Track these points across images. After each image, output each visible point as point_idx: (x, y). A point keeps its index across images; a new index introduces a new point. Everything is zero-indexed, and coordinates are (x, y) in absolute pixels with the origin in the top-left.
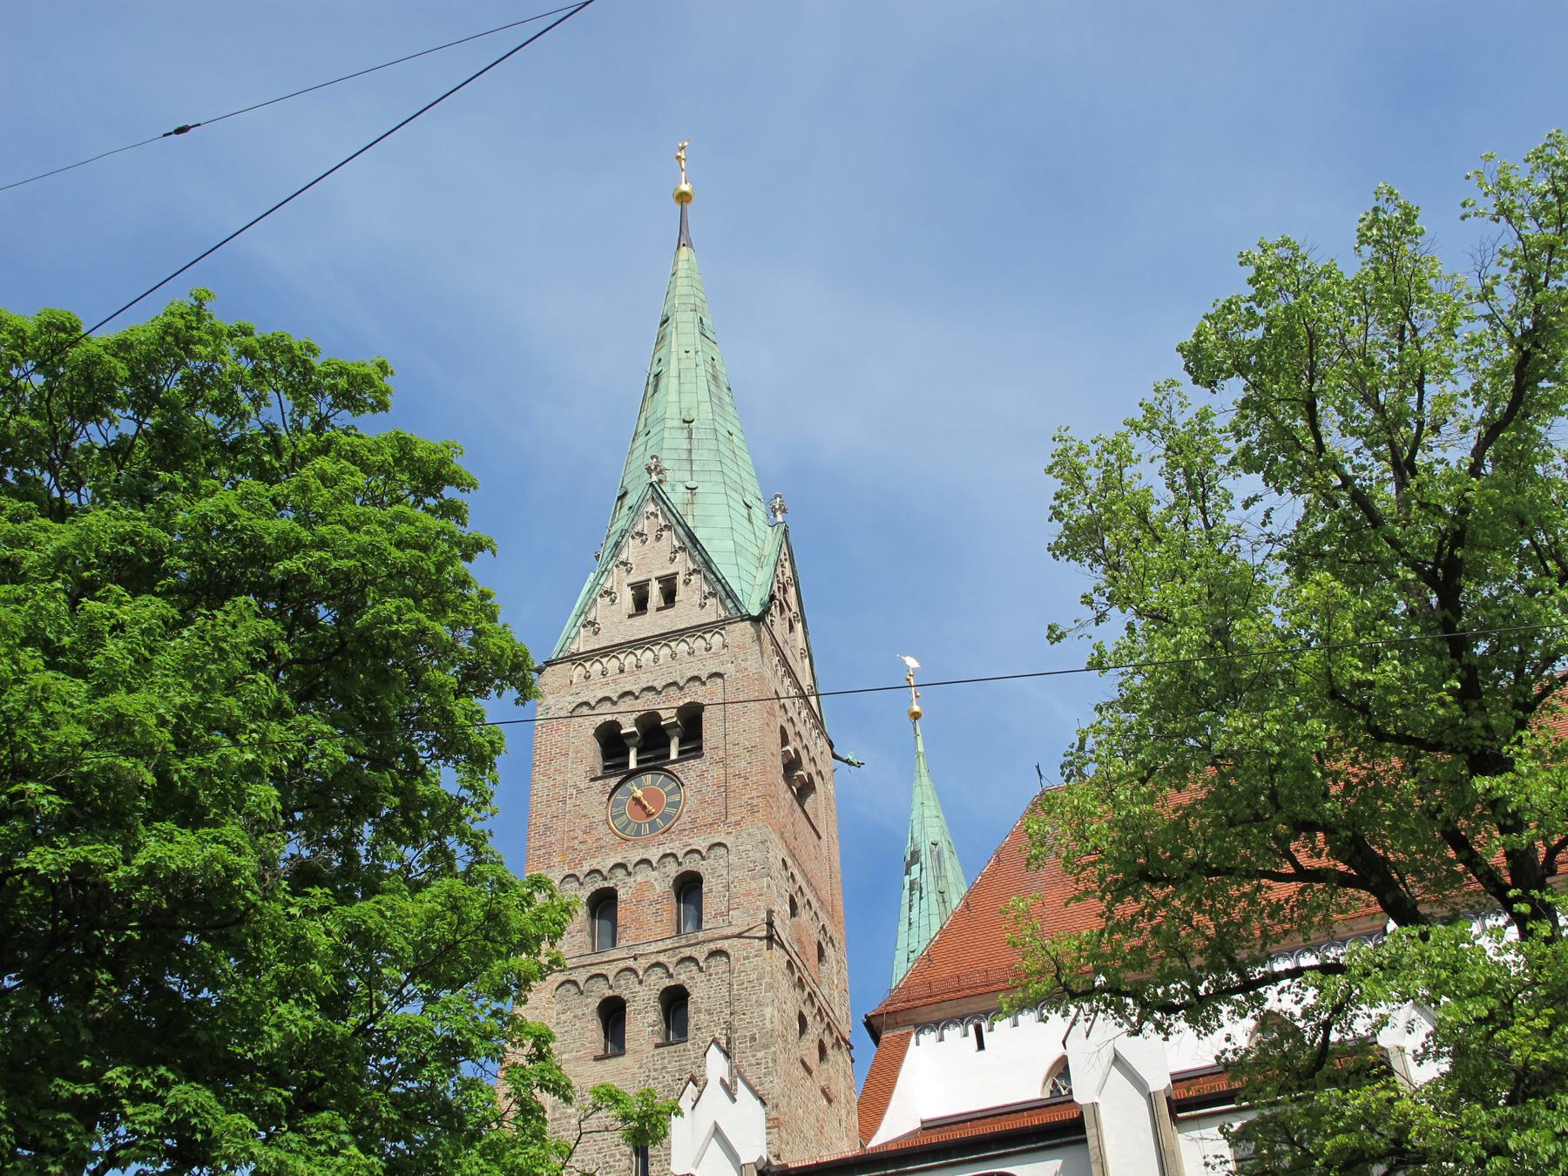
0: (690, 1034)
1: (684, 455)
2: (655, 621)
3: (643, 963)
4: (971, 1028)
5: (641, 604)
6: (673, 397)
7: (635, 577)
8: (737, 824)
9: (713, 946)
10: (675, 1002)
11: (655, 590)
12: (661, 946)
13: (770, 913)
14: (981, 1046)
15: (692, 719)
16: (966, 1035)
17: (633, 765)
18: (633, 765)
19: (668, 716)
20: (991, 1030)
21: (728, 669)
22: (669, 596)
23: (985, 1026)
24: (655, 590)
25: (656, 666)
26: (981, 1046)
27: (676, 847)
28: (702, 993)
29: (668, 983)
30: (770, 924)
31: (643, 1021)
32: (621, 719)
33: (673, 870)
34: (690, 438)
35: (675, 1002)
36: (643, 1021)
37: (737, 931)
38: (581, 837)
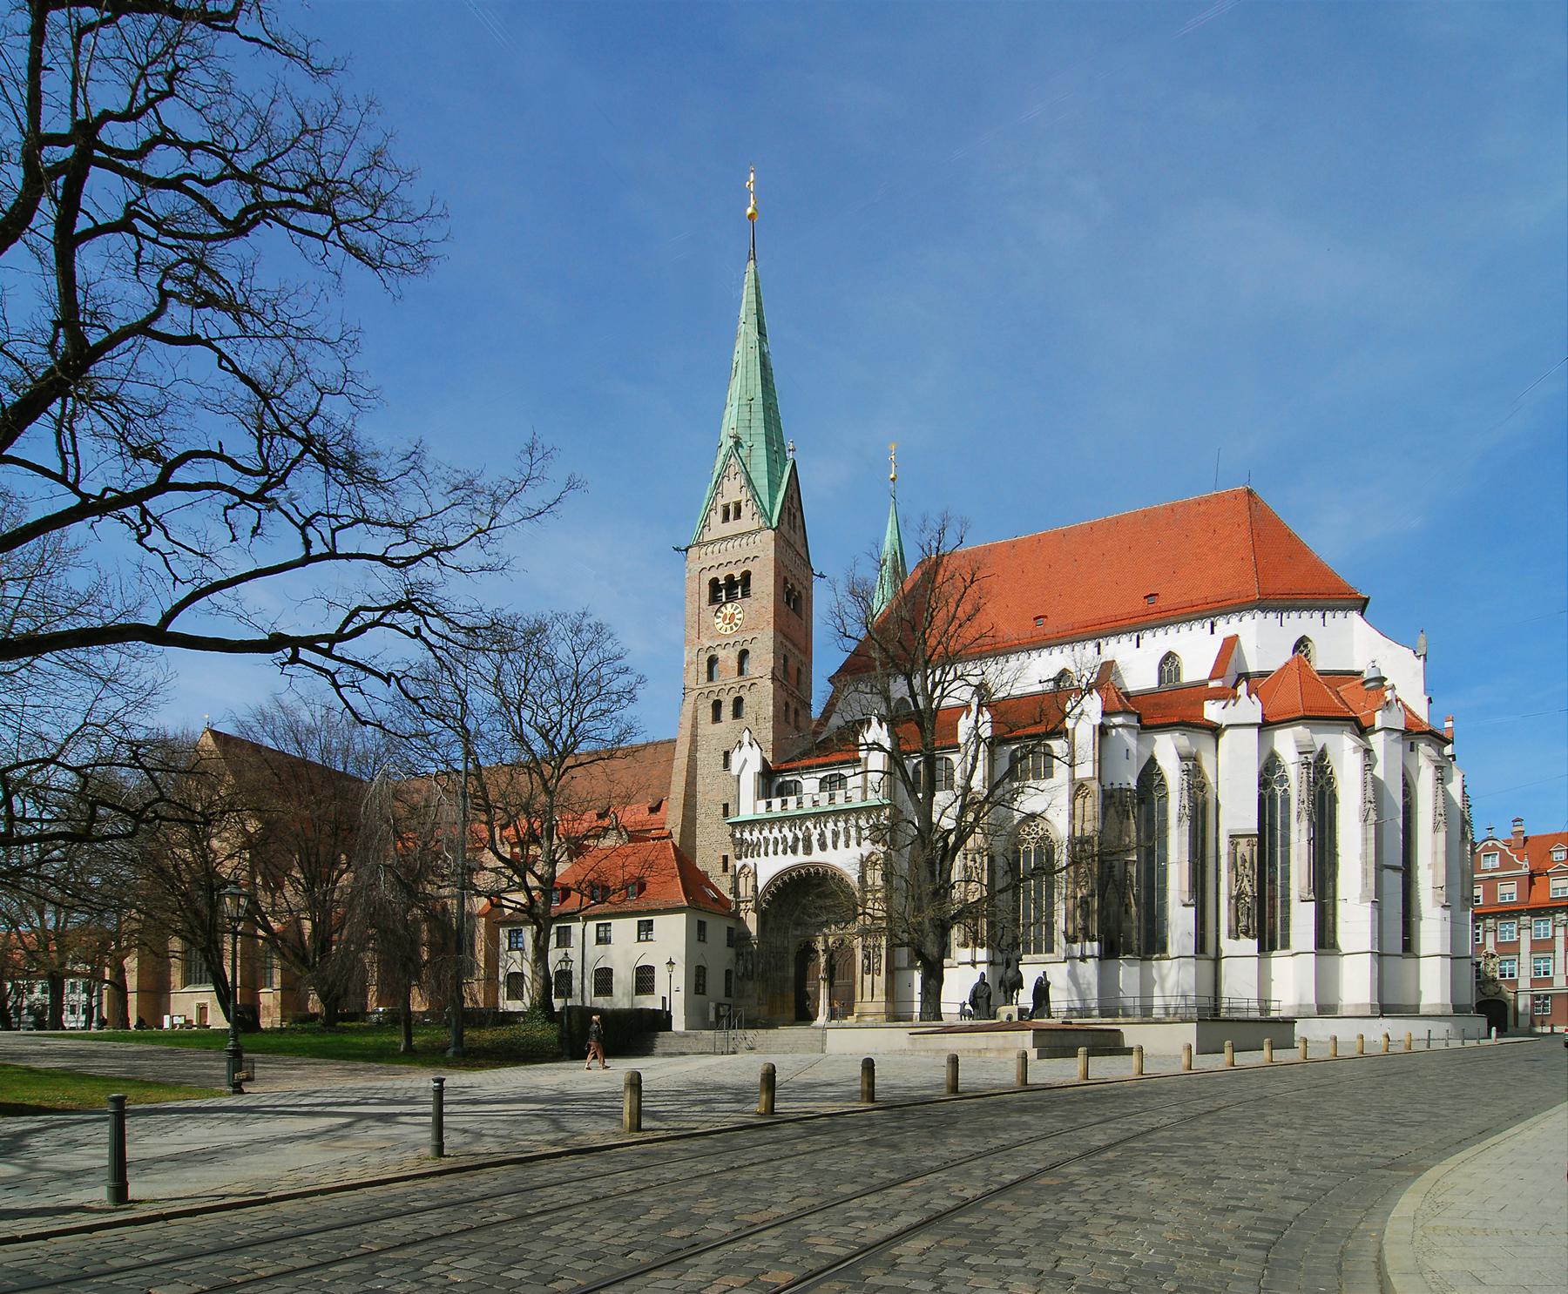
2: (733, 527)
3: (728, 687)
5: (726, 518)
7: (724, 502)
9: (752, 681)
10: (738, 702)
11: (732, 508)
12: (734, 680)
15: (747, 576)
17: (724, 600)
18: (724, 600)
19: (737, 577)
21: (761, 554)
22: (738, 515)
24: (732, 508)
25: (734, 551)
27: (739, 638)
28: (748, 700)
29: (737, 695)
31: (727, 711)
33: (739, 648)
35: (738, 702)
36: (727, 711)
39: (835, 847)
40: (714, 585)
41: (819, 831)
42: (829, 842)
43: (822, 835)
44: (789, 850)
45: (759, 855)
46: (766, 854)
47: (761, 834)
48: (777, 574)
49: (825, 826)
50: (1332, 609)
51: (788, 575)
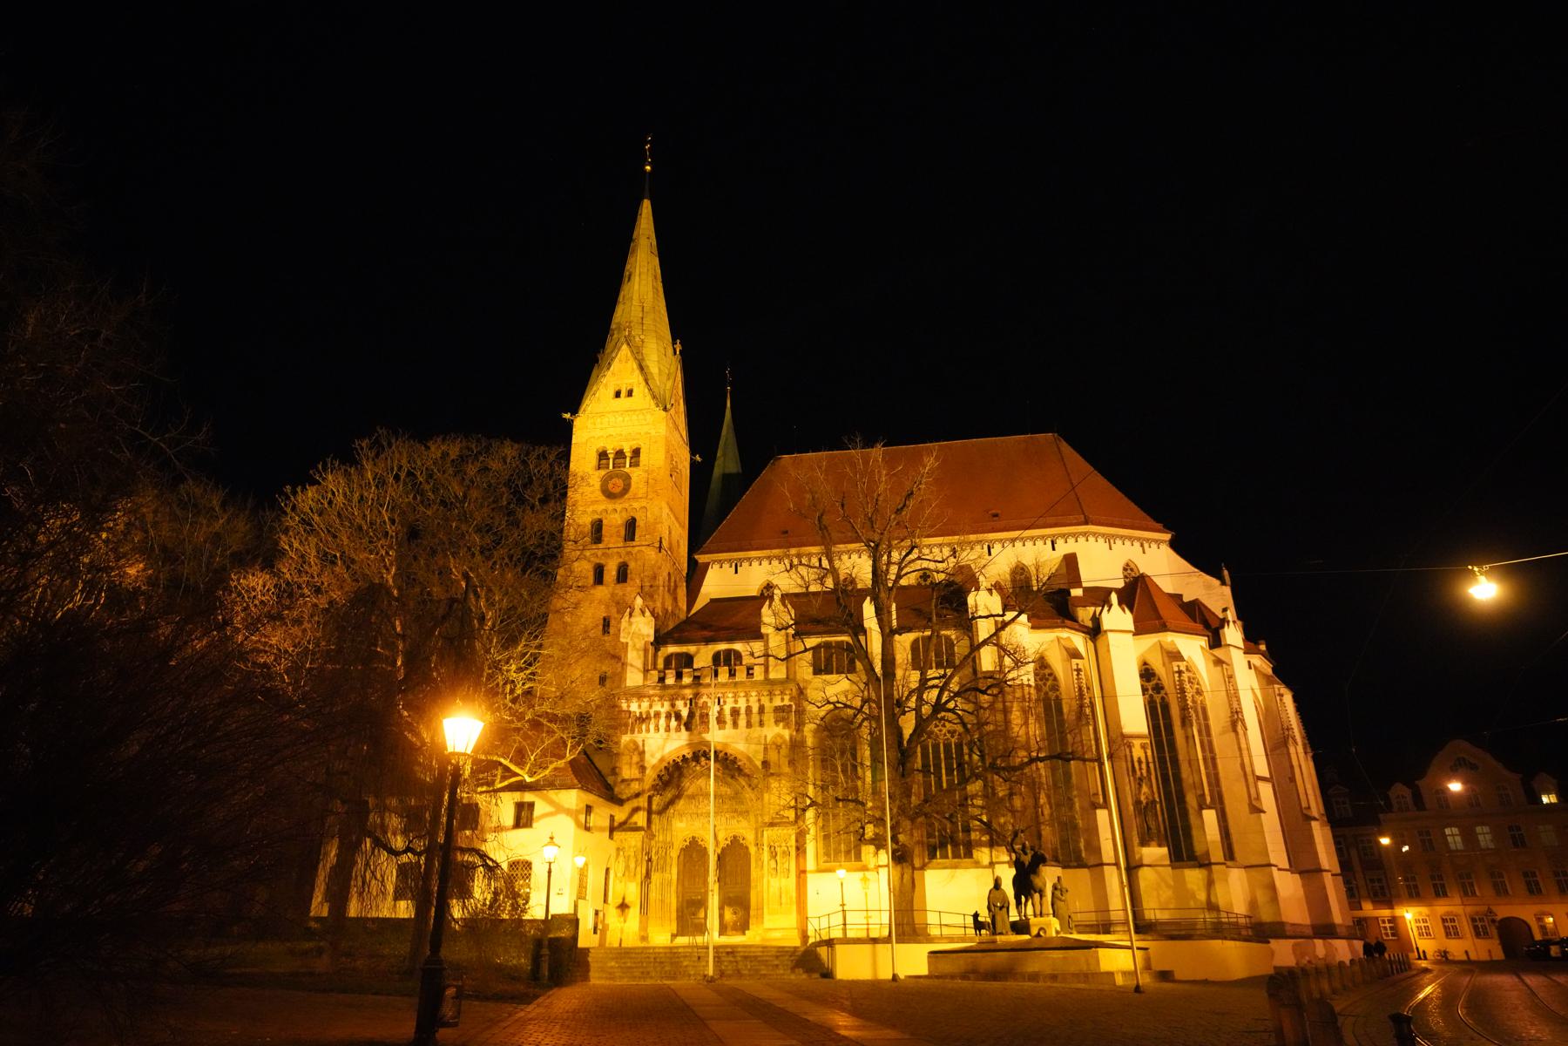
0: (628, 581)
1: (640, 321)
2: (624, 401)
4: (734, 565)
6: (636, 287)
8: (651, 499)
13: (661, 538)
14: (736, 572)
15: (636, 452)
16: (731, 567)
20: (741, 566)
22: (630, 393)
23: (739, 565)
26: (736, 572)
28: (632, 565)
30: (661, 542)
32: (608, 448)
34: (643, 311)
37: (647, 543)
38: (589, 495)
39: (735, 725)
40: (603, 455)
41: (717, 708)
42: (728, 718)
43: (721, 712)
44: (683, 728)
45: (648, 730)
46: (657, 729)
47: (651, 706)
48: (667, 452)
49: (725, 702)
50: (1149, 541)
51: (674, 453)
